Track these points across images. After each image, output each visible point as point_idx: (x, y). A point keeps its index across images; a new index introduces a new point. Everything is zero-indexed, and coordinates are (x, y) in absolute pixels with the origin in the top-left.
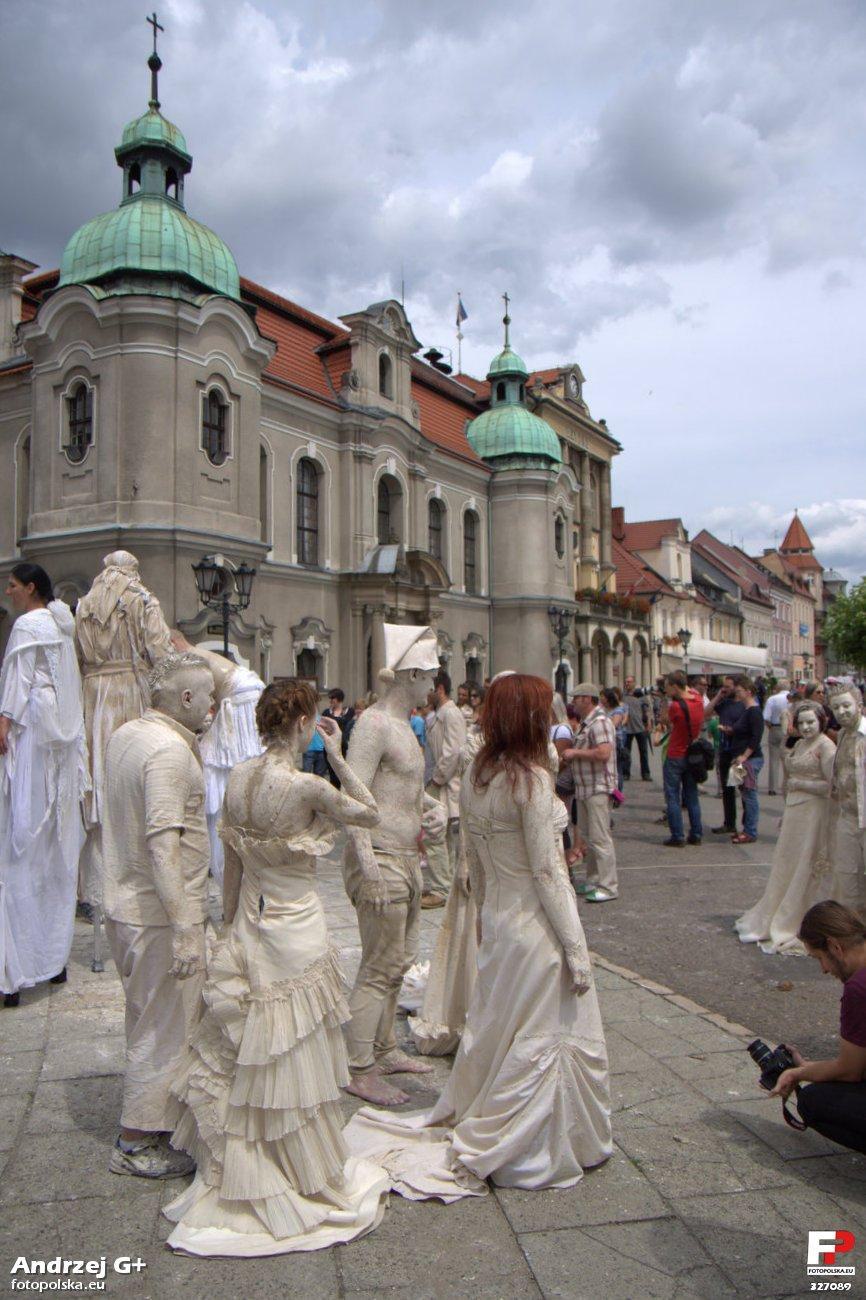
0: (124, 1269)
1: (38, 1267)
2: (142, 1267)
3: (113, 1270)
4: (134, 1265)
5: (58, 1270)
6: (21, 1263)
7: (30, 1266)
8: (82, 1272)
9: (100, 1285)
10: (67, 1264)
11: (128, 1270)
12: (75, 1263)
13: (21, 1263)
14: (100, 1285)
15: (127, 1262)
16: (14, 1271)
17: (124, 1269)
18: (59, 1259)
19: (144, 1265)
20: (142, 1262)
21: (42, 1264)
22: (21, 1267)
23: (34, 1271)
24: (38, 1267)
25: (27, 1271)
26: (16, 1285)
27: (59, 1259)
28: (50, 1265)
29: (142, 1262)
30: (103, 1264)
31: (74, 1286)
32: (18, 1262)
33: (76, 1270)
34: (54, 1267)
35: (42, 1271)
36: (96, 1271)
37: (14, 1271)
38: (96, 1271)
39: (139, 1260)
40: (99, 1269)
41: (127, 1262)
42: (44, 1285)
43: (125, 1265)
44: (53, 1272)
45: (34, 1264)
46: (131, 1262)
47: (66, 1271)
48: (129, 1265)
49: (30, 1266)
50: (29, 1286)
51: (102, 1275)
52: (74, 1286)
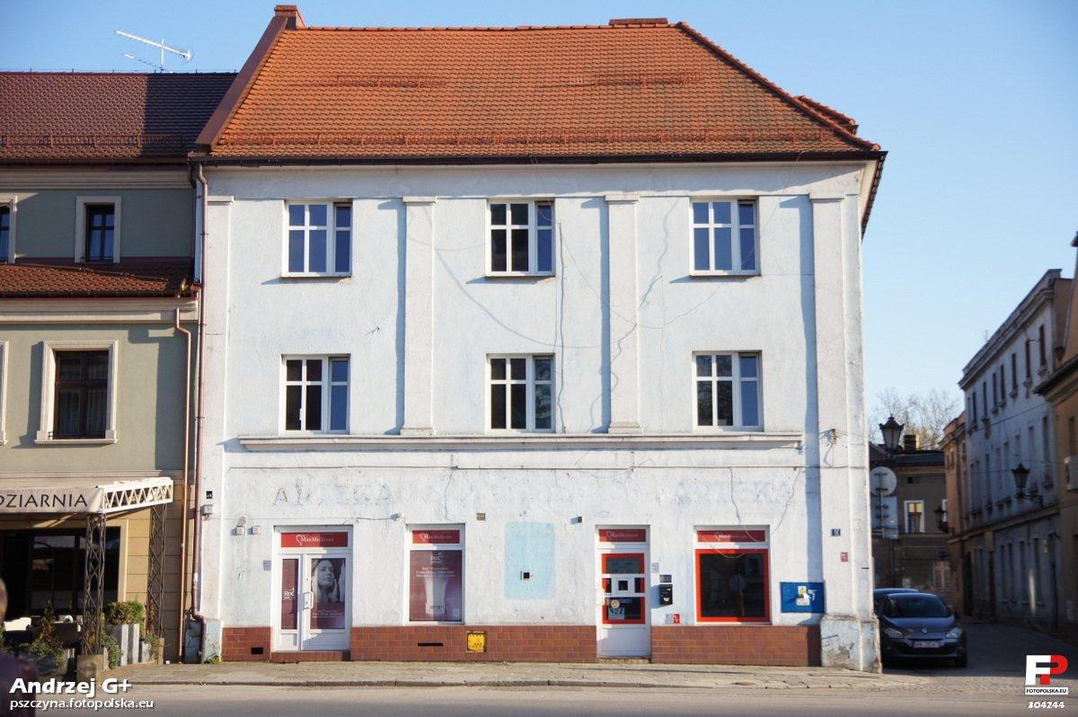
0: (112, 689)
1: (34, 688)
2: (127, 688)
3: (101, 689)
4: (120, 685)
5: (52, 690)
6: (18, 684)
7: (27, 688)
8: (73, 691)
9: (149, 704)
10: (60, 684)
11: (115, 690)
12: (67, 683)
13: (18, 684)
14: (149, 704)
15: (114, 683)
16: (12, 691)
17: (112, 689)
18: (53, 680)
19: (130, 685)
20: (127, 683)
21: (37, 684)
22: (19, 687)
23: (30, 691)
24: (34, 688)
25: (24, 691)
26: (73, 703)
27: (53, 680)
28: (46, 685)
29: (127, 683)
30: (93, 684)
31: (127, 704)
32: (16, 683)
33: (68, 690)
34: (49, 686)
35: (38, 691)
36: (86, 691)
37: (12, 691)
38: (86, 691)
39: (125, 681)
40: (89, 689)
41: (114, 683)
42: (98, 704)
43: (112, 686)
44: (48, 691)
45: (31, 684)
46: (117, 683)
47: (59, 690)
48: (116, 686)
49: (27, 688)
50: (86, 703)
51: (92, 694)
52: (127, 704)
